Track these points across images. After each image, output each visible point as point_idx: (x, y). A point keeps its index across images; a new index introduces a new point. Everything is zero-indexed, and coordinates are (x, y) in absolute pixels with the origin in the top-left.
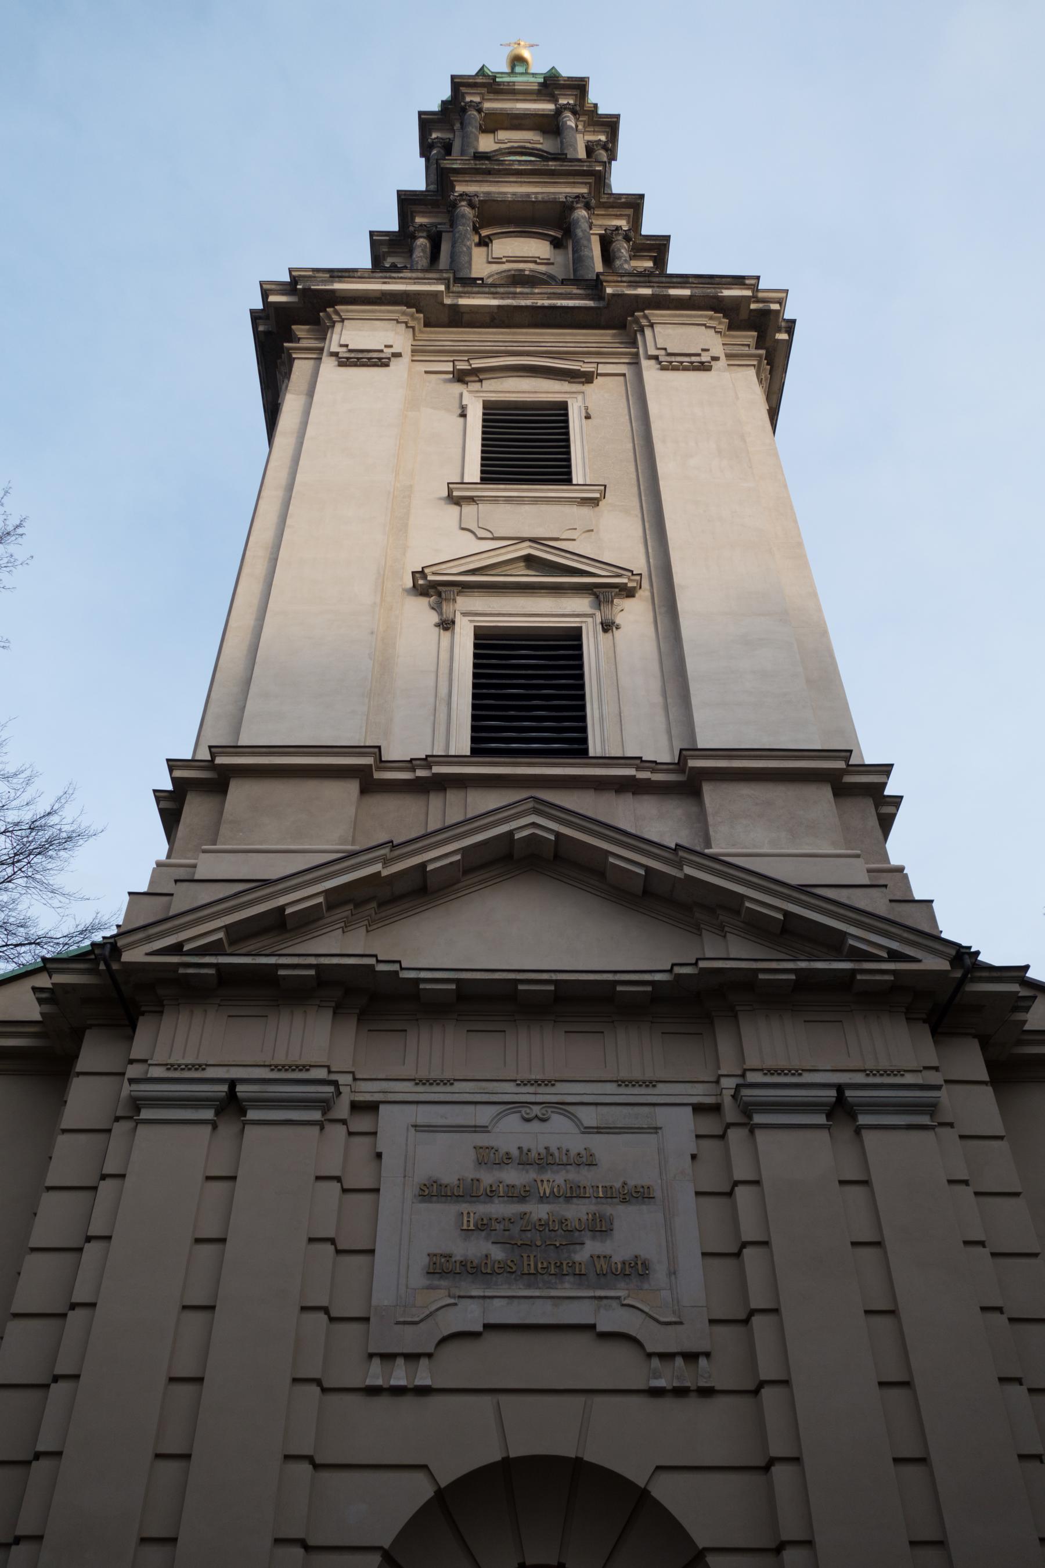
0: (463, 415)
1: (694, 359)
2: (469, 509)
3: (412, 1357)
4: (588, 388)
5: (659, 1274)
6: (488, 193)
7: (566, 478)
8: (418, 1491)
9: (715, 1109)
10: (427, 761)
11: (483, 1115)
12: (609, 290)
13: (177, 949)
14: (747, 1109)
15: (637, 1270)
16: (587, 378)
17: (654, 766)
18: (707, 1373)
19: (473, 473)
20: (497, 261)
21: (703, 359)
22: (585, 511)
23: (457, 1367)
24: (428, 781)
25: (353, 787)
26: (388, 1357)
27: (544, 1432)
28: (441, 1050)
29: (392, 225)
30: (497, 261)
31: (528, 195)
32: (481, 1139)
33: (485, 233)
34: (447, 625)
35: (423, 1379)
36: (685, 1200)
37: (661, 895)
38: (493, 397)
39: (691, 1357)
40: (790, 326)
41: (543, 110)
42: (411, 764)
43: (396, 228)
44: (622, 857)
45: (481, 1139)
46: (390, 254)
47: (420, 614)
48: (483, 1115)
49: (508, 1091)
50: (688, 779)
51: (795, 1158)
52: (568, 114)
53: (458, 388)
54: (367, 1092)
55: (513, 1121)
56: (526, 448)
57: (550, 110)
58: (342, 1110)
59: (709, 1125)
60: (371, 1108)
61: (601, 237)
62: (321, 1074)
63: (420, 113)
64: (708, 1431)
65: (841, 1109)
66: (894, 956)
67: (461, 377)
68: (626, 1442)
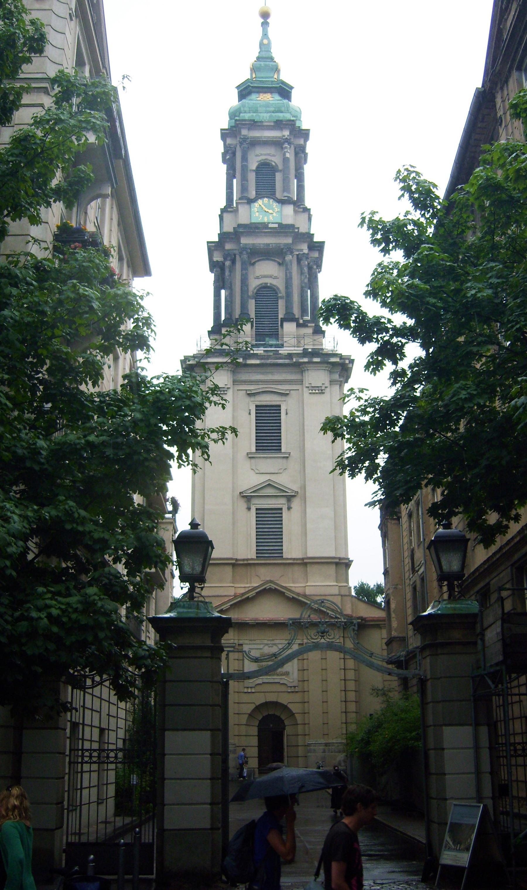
0: (250, 414)
1: (320, 388)
2: (253, 460)
3: (251, 687)
5: (291, 674)
7: (279, 449)
8: (253, 707)
9: (303, 644)
11: (261, 646)
12: (294, 360)
15: (287, 674)
17: (297, 559)
18: (297, 689)
19: (254, 449)
20: (257, 278)
21: (323, 388)
23: (259, 689)
25: (231, 567)
26: (248, 688)
27: (271, 698)
28: (254, 634)
29: (216, 239)
30: (257, 278)
31: (268, 245)
32: (262, 651)
33: (253, 261)
34: (249, 509)
35: (253, 691)
37: (295, 601)
38: (259, 403)
39: (295, 687)
40: (352, 361)
41: (272, 373)
42: (244, 560)
43: (217, 240)
44: (288, 594)
45: (262, 651)
46: (215, 250)
47: (242, 505)
48: (261, 646)
49: (266, 642)
50: (305, 563)
52: (286, 145)
53: (248, 399)
54: (241, 642)
55: (266, 647)
57: (279, 137)
58: (237, 647)
60: (242, 645)
61: (297, 255)
62: (232, 641)
63: (222, 130)
64: (297, 697)
66: (337, 618)
67: (249, 395)
68: (284, 699)
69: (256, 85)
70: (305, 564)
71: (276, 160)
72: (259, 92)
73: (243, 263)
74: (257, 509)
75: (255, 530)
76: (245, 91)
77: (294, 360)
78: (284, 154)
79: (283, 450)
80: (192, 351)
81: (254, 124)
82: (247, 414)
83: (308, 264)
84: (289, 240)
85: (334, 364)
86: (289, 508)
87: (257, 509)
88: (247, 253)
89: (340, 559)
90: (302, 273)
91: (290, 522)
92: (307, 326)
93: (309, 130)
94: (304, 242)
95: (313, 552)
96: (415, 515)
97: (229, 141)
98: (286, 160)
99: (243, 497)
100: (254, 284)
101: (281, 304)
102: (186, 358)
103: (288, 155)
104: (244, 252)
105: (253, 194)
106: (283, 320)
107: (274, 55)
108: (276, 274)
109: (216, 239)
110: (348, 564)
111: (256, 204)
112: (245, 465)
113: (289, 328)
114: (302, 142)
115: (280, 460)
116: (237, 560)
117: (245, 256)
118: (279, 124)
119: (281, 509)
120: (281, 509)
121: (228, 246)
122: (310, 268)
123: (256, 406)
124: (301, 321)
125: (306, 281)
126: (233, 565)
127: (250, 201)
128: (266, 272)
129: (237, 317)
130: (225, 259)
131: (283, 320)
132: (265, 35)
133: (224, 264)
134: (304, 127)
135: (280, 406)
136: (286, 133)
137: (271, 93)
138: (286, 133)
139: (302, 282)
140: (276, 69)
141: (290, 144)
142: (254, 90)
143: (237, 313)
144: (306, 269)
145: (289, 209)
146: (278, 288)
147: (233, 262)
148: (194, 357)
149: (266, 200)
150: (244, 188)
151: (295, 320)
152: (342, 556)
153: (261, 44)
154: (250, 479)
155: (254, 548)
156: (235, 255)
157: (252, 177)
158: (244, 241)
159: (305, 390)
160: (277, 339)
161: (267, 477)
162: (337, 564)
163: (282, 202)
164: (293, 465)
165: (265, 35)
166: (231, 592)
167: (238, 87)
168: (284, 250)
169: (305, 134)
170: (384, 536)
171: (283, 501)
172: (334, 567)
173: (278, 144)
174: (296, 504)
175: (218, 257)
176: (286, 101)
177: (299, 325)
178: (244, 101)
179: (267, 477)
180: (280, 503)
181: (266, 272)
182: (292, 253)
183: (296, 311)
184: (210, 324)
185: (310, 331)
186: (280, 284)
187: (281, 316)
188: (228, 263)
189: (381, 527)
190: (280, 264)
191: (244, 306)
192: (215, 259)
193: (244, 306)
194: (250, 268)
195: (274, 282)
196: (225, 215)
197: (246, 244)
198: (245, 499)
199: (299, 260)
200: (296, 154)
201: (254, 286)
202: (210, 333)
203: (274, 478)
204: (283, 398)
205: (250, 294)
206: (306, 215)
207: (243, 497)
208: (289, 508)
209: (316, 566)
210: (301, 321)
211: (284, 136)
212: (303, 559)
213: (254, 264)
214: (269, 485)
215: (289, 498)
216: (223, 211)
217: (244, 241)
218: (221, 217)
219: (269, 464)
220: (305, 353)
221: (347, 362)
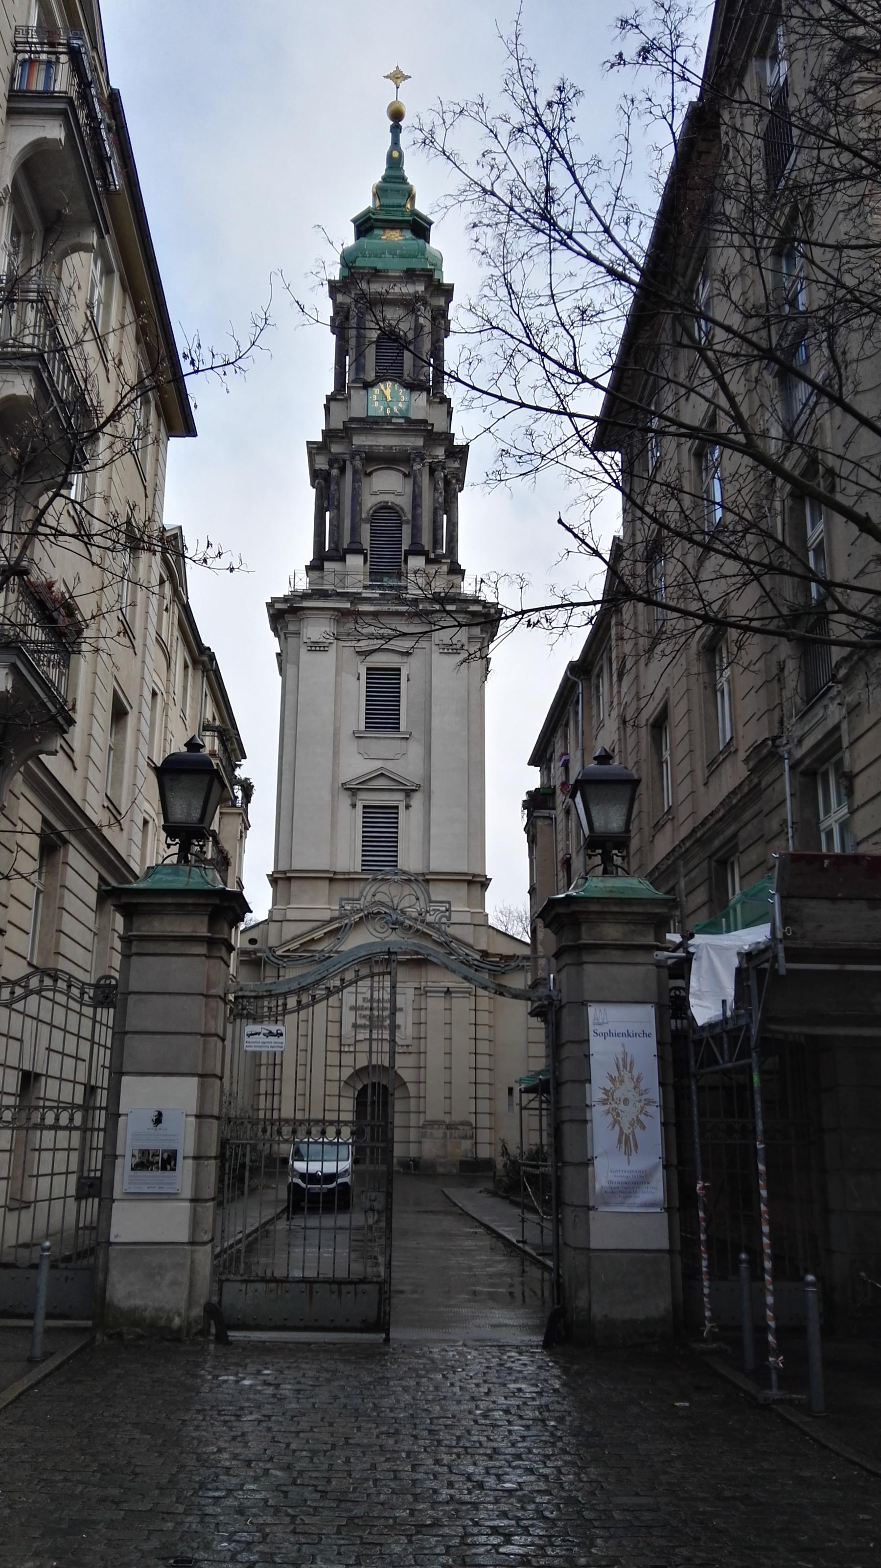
2: (361, 741)
4: (411, 659)
5: (403, 1028)
6: (370, 446)
10: (349, 873)
12: (421, 607)
13: (288, 951)
14: (426, 992)
16: (408, 654)
18: (411, 1049)
19: (362, 727)
22: (404, 742)
24: (349, 879)
25: (327, 882)
29: (319, 438)
31: (391, 447)
34: (354, 806)
36: (410, 1011)
42: (344, 873)
47: (345, 800)
50: (426, 879)
51: (435, 1004)
56: (383, 707)
59: (417, 992)
65: (448, 992)
69: (380, 217)
70: (427, 881)
71: (405, 327)
72: (384, 228)
73: (355, 472)
74: (364, 807)
75: (361, 834)
76: (365, 225)
77: (421, 607)
78: (417, 320)
79: (402, 729)
80: (283, 591)
81: (376, 274)
82: (355, 679)
83: (445, 476)
84: (420, 442)
85: (474, 614)
86: (408, 807)
87: (364, 807)
88: (361, 459)
89: (474, 876)
90: (436, 489)
91: (409, 824)
92: (440, 562)
93: (452, 286)
94: (441, 445)
95: (439, 864)
96: (573, 811)
97: (340, 298)
98: (418, 328)
99: (347, 789)
100: (369, 502)
101: (406, 530)
102: (275, 600)
103: (421, 320)
104: (358, 457)
105: (371, 376)
106: (408, 553)
107: (407, 174)
108: (399, 489)
109: (319, 438)
110: (484, 883)
111: (376, 390)
112: (349, 747)
113: (416, 562)
114: (442, 302)
115: (398, 742)
116: (335, 873)
117: (358, 463)
118: (410, 275)
119: (397, 807)
120: (397, 807)
121: (335, 449)
122: (447, 483)
123: (368, 669)
124: (432, 556)
125: (441, 500)
126: (331, 880)
127: (367, 386)
128: (387, 486)
129: (345, 546)
130: (331, 466)
131: (408, 553)
132: (396, 143)
133: (329, 474)
134: (446, 280)
135: (399, 669)
136: (421, 288)
137: (401, 229)
138: (421, 288)
139: (435, 501)
140: (410, 195)
141: (425, 304)
142: (379, 224)
143: (346, 542)
144: (441, 484)
145: (421, 399)
146: (402, 509)
147: (342, 470)
148: (285, 599)
149: (389, 384)
150: (359, 366)
151: (425, 553)
152: (477, 871)
153: (390, 157)
154: (356, 765)
155: (359, 858)
156: (344, 461)
157: (371, 354)
158: (359, 440)
159: (434, 648)
160: (400, 580)
161: (379, 764)
162: (469, 882)
163: (413, 386)
164: (415, 749)
165: (396, 143)
166: (327, 915)
167: (354, 221)
168: (412, 456)
169: (447, 292)
170: (532, 841)
171: (400, 796)
172: (465, 885)
173: (410, 305)
174: (417, 800)
175: (322, 463)
176: (421, 241)
177: (429, 561)
178: (362, 239)
179: (379, 764)
180: (395, 799)
181: (387, 486)
182: (423, 459)
183: (426, 541)
184: (308, 556)
185: (445, 568)
186: (404, 502)
187: (405, 547)
188: (335, 472)
189: (527, 829)
190: (406, 476)
191: (355, 530)
192: (317, 467)
193: (355, 530)
194: (365, 481)
195: (398, 500)
196: (333, 405)
197: (360, 446)
198: (349, 793)
199: (432, 472)
200: (434, 319)
201: (369, 505)
202: (308, 569)
203: (389, 765)
204: (405, 659)
205: (364, 515)
206: (444, 407)
207: (347, 789)
208: (408, 807)
209: (442, 884)
210: (432, 556)
211: (417, 292)
212: (423, 874)
213: (370, 475)
214: (382, 774)
215: (408, 793)
216: (330, 399)
217: (359, 440)
218: (327, 408)
219: (383, 746)
220: (437, 598)
221: (493, 611)
